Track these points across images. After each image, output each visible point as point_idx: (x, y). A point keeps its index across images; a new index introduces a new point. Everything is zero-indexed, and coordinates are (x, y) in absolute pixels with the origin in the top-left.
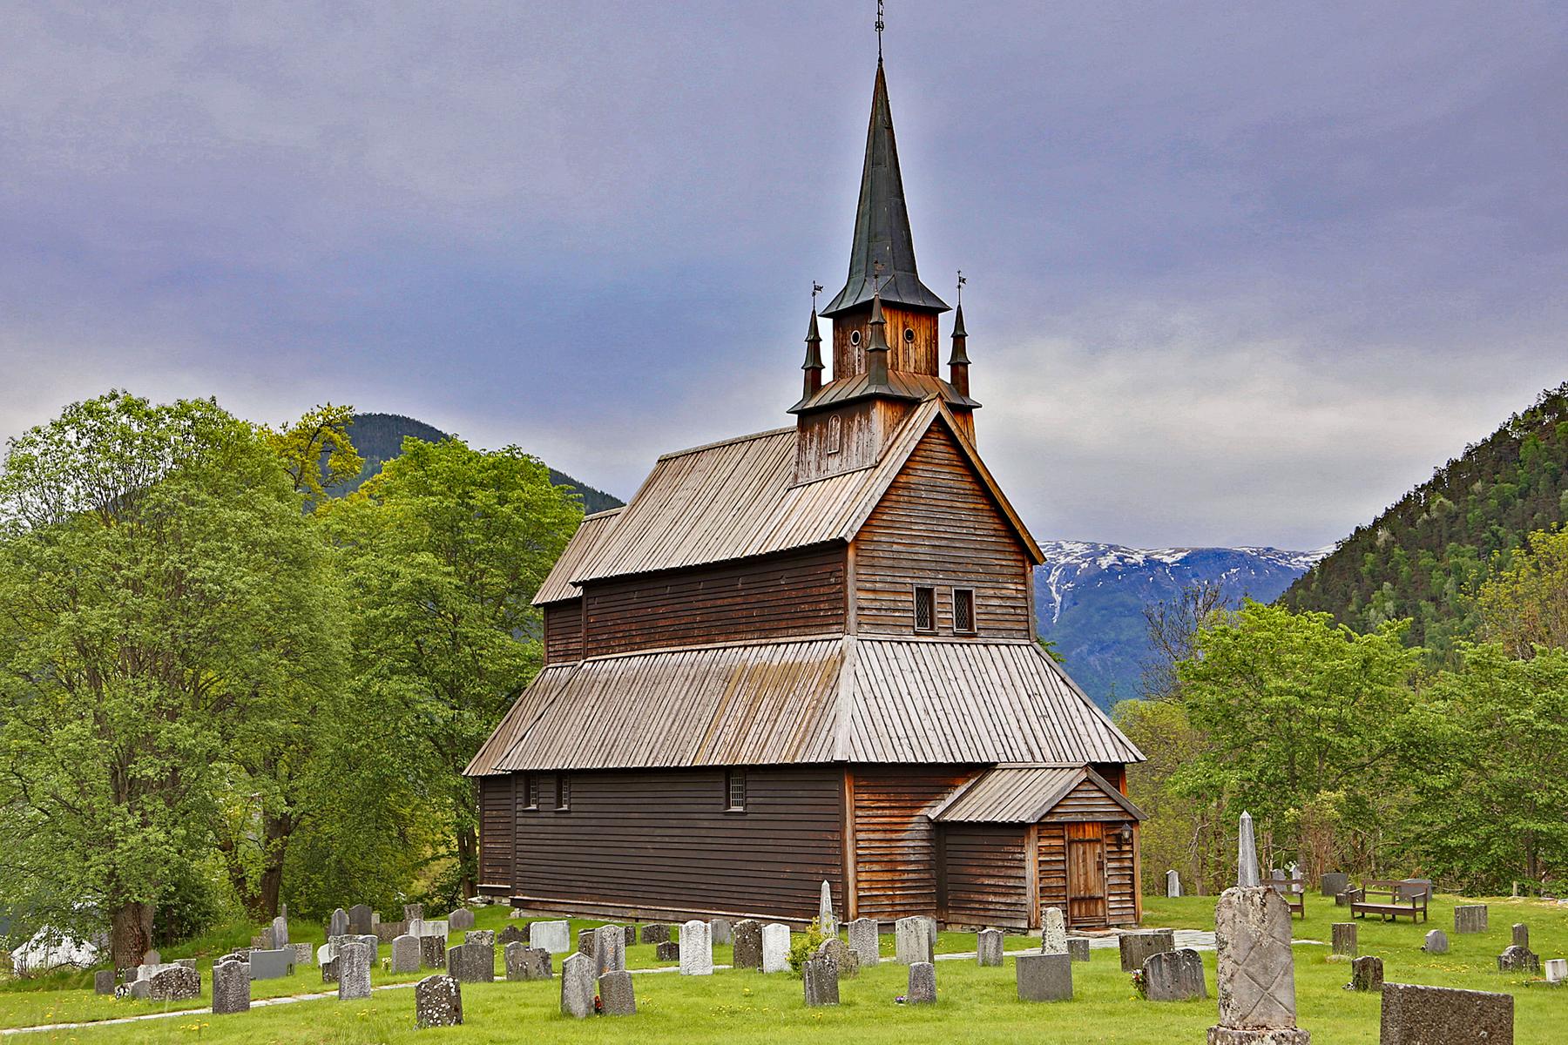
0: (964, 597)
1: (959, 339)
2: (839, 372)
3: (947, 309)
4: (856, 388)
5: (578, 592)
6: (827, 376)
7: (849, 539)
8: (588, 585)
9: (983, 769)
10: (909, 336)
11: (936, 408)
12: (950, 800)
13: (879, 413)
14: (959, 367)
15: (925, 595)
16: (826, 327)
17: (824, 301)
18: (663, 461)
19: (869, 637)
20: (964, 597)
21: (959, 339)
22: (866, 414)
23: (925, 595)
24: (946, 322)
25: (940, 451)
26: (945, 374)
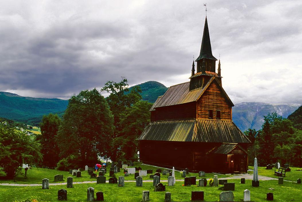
1: (219, 65)
3: (217, 60)
4: (200, 74)
6: (196, 72)
14: (219, 69)
16: (196, 63)
19: (200, 119)
21: (219, 65)
24: (217, 63)
25: (214, 86)
26: (217, 72)
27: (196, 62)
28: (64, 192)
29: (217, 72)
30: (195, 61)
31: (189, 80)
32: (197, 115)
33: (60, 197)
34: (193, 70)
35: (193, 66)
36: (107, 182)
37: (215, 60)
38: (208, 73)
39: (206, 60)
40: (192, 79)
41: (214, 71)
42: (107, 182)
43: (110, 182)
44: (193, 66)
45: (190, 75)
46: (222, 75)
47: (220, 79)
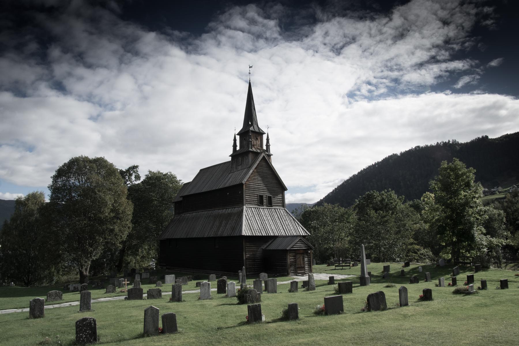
1: (268, 140)
3: (265, 133)
4: (245, 150)
5: (181, 199)
6: (238, 148)
8: (184, 197)
12: (267, 244)
13: (251, 156)
14: (268, 146)
16: (238, 138)
18: (201, 170)
21: (268, 140)
23: (261, 197)
24: (265, 137)
25: (264, 164)
26: (265, 148)
27: (239, 136)
28: (90, 323)
29: (265, 148)
30: (238, 134)
31: (230, 159)
32: (244, 201)
33: (82, 336)
34: (235, 146)
35: (235, 140)
36: (145, 295)
39: (250, 133)
42: (145, 295)
43: (148, 298)
44: (235, 140)
45: (231, 152)
46: (272, 151)
47: (269, 156)
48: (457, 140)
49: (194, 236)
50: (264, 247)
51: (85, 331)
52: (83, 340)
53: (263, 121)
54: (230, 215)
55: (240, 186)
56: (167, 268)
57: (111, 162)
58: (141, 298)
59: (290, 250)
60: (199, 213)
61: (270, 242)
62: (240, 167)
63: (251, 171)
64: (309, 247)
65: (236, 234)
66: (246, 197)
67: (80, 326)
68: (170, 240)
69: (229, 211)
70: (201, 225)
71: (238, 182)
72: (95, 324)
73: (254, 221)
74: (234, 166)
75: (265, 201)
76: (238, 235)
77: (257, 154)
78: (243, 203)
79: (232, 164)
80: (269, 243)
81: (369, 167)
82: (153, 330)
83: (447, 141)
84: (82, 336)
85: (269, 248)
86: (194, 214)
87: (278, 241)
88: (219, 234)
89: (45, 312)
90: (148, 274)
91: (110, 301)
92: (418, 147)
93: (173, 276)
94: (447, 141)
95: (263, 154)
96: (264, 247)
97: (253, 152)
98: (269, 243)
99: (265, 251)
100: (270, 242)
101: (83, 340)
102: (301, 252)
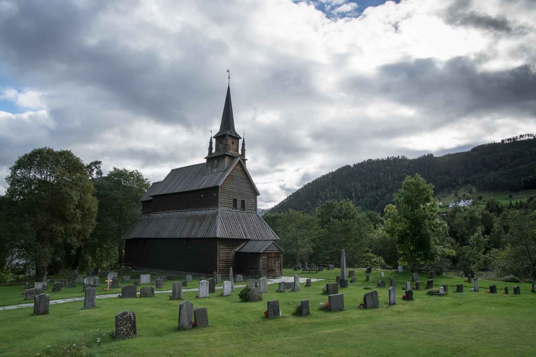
0: (243, 202)
1: (243, 144)
2: (216, 150)
5: (151, 198)
7: (220, 186)
8: (153, 196)
9: (247, 240)
10: (233, 143)
11: (239, 159)
12: (240, 247)
13: (227, 160)
14: (243, 150)
15: (235, 200)
16: (214, 140)
17: (214, 134)
18: (172, 171)
20: (243, 202)
21: (243, 144)
22: (224, 159)
23: (235, 200)
24: (241, 141)
25: (239, 168)
31: (205, 161)
32: (219, 203)
33: (122, 330)
34: (210, 148)
35: (211, 143)
36: (138, 293)
37: (237, 138)
38: (231, 152)
40: (209, 159)
41: (237, 151)
42: (138, 293)
45: (206, 154)
46: (247, 156)
47: (244, 160)
48: (406, 156)
49: (165, 237)
50: (237, 249)
51: (126, 324)
52: (124, 334)
53: (239, 127)
54: (204, 217)
55: (216, 188)
56: (133, 268)
57: (78, 157)
58: (135, 296)
59: (263, 253)
60: (171, 214)
61: (243, 245)
62: (215, 170)
63: (227, 175)
64: (280, 250)
65: (211, 235)
66: (221, 200)
67: (121, 320)
68: (137, 240)
69: (203, 212)
70: (171, 225)
71: (213, 184)
72: (135, 318)
73: (224, 224)
74: (209, 168)
75: (239, 205)
76: (212, 237)
77: (232, 158)
78: (217, 205)
79: (207, 167)
80: (242, 246)
81: (324, 176)
82: (188, 323)
83: (397, 157)
84: (122, 330)
85: (242, 251)
86: (165, 214)
87: (250, 244)
88: (192, 235)
89: (50, 309)
90: (117, 273)
91: (76, 302)
92: (371, 160)
93: (148, 276)
94: (397, 157)
95: (239, 159)
96: (237, 249)
97: (229, 156)
98: (242, 246)
99: (238, 254)
100: (243, 245)
101: (124, 334)
102: (273, 255)
